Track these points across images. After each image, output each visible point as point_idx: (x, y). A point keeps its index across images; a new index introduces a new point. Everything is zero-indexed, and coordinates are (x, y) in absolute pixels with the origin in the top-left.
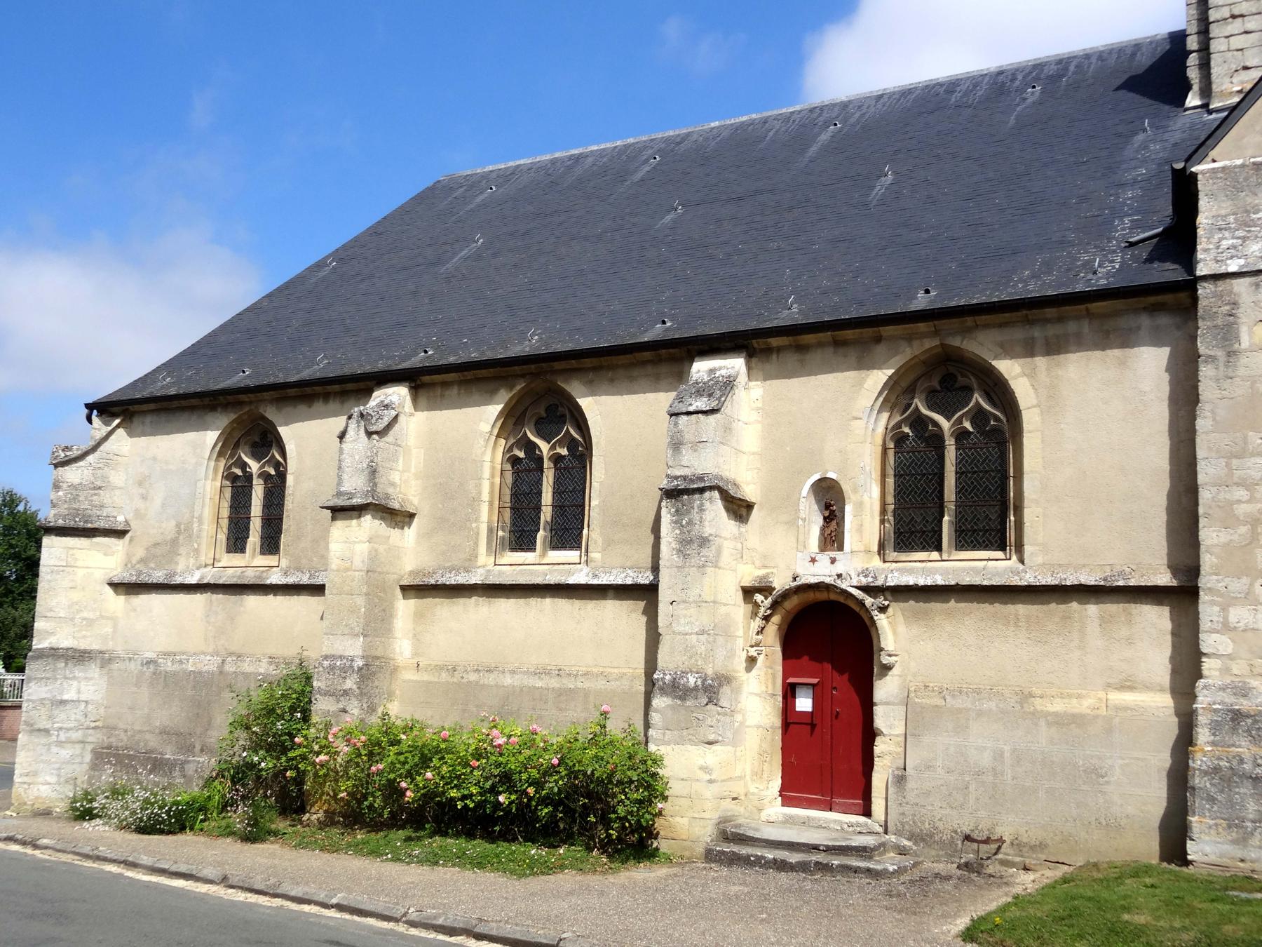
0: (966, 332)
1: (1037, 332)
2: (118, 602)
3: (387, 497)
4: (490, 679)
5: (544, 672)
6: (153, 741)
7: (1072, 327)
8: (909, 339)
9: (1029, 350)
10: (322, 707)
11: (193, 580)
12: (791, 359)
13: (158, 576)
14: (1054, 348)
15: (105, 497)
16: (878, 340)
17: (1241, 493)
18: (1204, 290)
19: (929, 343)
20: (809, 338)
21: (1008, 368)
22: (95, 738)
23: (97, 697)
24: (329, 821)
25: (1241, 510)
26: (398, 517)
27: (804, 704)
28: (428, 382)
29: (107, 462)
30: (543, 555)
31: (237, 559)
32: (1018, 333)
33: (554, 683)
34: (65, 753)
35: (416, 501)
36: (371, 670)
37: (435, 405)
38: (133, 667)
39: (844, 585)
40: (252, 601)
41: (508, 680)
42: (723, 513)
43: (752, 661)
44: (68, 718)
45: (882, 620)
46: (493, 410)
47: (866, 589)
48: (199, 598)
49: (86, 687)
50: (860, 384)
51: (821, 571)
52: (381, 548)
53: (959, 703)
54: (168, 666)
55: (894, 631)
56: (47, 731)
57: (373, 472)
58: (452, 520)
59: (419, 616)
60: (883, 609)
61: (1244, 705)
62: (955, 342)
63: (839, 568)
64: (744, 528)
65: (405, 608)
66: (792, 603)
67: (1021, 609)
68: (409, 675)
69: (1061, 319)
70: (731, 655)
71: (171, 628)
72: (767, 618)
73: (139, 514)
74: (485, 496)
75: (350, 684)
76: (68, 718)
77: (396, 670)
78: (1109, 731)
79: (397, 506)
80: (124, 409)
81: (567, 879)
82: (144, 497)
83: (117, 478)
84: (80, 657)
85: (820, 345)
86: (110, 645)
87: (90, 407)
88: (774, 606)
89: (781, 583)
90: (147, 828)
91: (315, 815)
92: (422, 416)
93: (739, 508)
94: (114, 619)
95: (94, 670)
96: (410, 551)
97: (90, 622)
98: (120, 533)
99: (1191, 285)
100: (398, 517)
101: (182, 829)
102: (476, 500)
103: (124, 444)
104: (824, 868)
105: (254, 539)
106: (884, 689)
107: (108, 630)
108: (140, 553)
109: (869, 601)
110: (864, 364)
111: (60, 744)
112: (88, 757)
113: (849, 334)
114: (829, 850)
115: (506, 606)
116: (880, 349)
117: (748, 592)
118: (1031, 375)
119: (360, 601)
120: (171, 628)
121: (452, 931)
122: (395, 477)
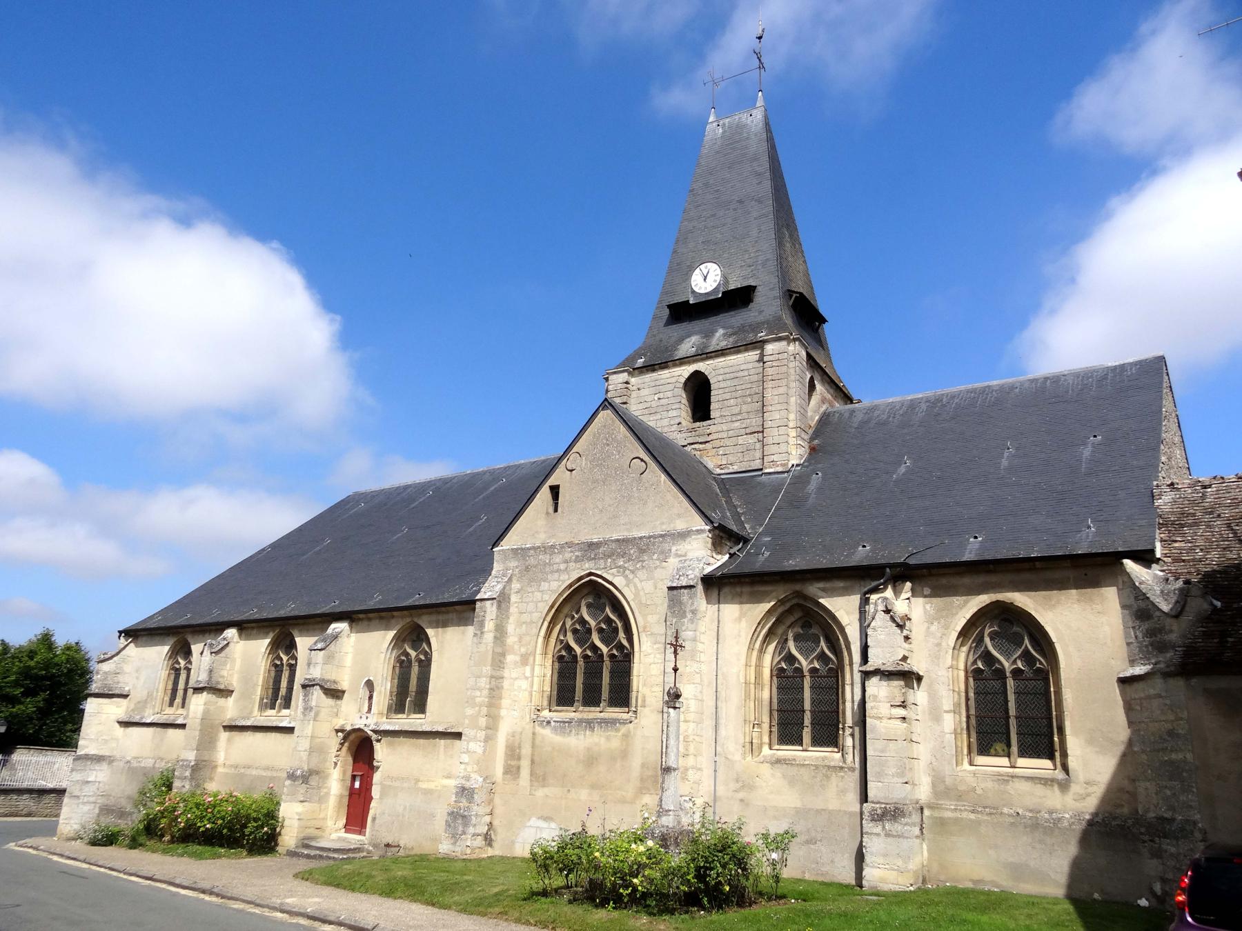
0: (420, 616)
1: (441, 617)
2: (120, 731)
3: (218, 683)
4: (248, 772)
5: (267, 768)
6: (123, 802)
7: (450, 616)
8: (402, 617)
9: (437, 625)
10: (177, 784)
11: (148, 721)
12: (366, 623)
13: (137, 719)
14: (445, 625)
15: (120, 678)
16: (393, 617)
17: (478, 693)
18: (478, 605)
19: (408, 620)
20: (371, 615)
21: (430, 632)
22: (101, 801)
23: (105, 780)
24: (172, 842)
25: (478, 700)
26: (225, 693)
27: (357, 785)
28: (246, 627)
29: (124, 661)
30: (279, 711)
31: (169, 711)
32: (434, 617)
33: (269, 774)
34: (86, 808)
35: (235, 684)
36: (200, 768)
37: (248, 638)
38: (122, 764)
39: (366, 729)
40: (171, 731)
41: (254, 772)
42: (323, 696)
43: (336, 764)
44: (89, 790)
45: (377, 747)
46: (267, 641)
47: (374, 731)
48: (151, 730)
49: (100, 775)
50: (384, 638)
51: (359, 724)
52: (212, 708)
53: (397, 784)
54: (135, 764)
55: (381, 751)
56: (78, 797)
57: (211, 671)
58: (246, 696)
59: (229, 740)
60: (378, 741)
61: (468, 785)
62: (416, 620)
63: (367, 722)
64: (339, 702)
65: (224, 736)
66: (352, 737)
67: (421, 741)
68: (220, 770)
69: (448, 612)
70: (325, 760)
72: (342, 744)
73: (135, 687)
74: (260, 683)
75: (188, 774)
76: (89, 790)
77: (216, 767)
78: (439, 797)
79: (222, 687)
80: (135, 634)
81: (224, 861)
82: (137, 678)
83: (127, 668)
84: (99, 759)
85: (375, 618)
86: (115, 753)
87: (120, 632)
88: (345, 738)
89: (348, 728)
90: (94, 843)
91: (167, 838)
92: (242, 642)
93: (335, 693)
94: (117, 740)
95: (104, 766)
96: (230, 709)
97: (106, 741)
98: (125, 696)
99: (474, 602)
100: (225, 693)
101: (111, 844)
102: (256, 685)
103: (133, 651)
104: (321, 856)
105: (178, 700)
106: (377, 777)
107: (114, 745)
108: (132, 706)
109: (374, 737)
110: (387, 628)
111: (84, 803)
112: (97, 811)
113: (383, 614)
114: (336, 851)
115: (259, 736)
116: (393, 621)
117: (337, 731)
118: (436, 636)
119: (197, 733)
120: (138, 744)
121: (131, 875)
122: (225, 673)
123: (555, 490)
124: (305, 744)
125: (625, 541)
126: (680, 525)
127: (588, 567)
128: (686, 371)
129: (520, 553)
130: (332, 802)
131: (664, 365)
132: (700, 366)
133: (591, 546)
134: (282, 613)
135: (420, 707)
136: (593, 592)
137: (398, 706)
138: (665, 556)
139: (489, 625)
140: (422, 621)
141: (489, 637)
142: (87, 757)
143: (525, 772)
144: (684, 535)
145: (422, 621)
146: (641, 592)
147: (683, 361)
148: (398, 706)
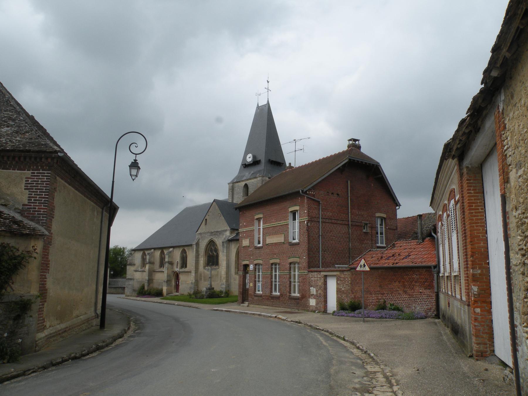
71: (138, 276)
84: (131, 279)
123: (206, 220)
124: (166, 275)
125: (217, 232)
126: (226, 228)
127: (211, 237)
128: (243, 184)
129: (200, 234)
130: (173, 286)
131: (239, 182)
132: (247, 182)
133: (212, 233)
134: (162, 246)
135: (186, 267)
136: (212, 243)
137: (182, 267)
138: (223, 234)
139: (195, 250)
140: (186, 248)
141: (195, 252)
142: (128, 279)
143: (203, 279)
144: (226, 231)
145: (186, 248)
146: (219, 241)
147: (243, 181)
148: (182, 267)
